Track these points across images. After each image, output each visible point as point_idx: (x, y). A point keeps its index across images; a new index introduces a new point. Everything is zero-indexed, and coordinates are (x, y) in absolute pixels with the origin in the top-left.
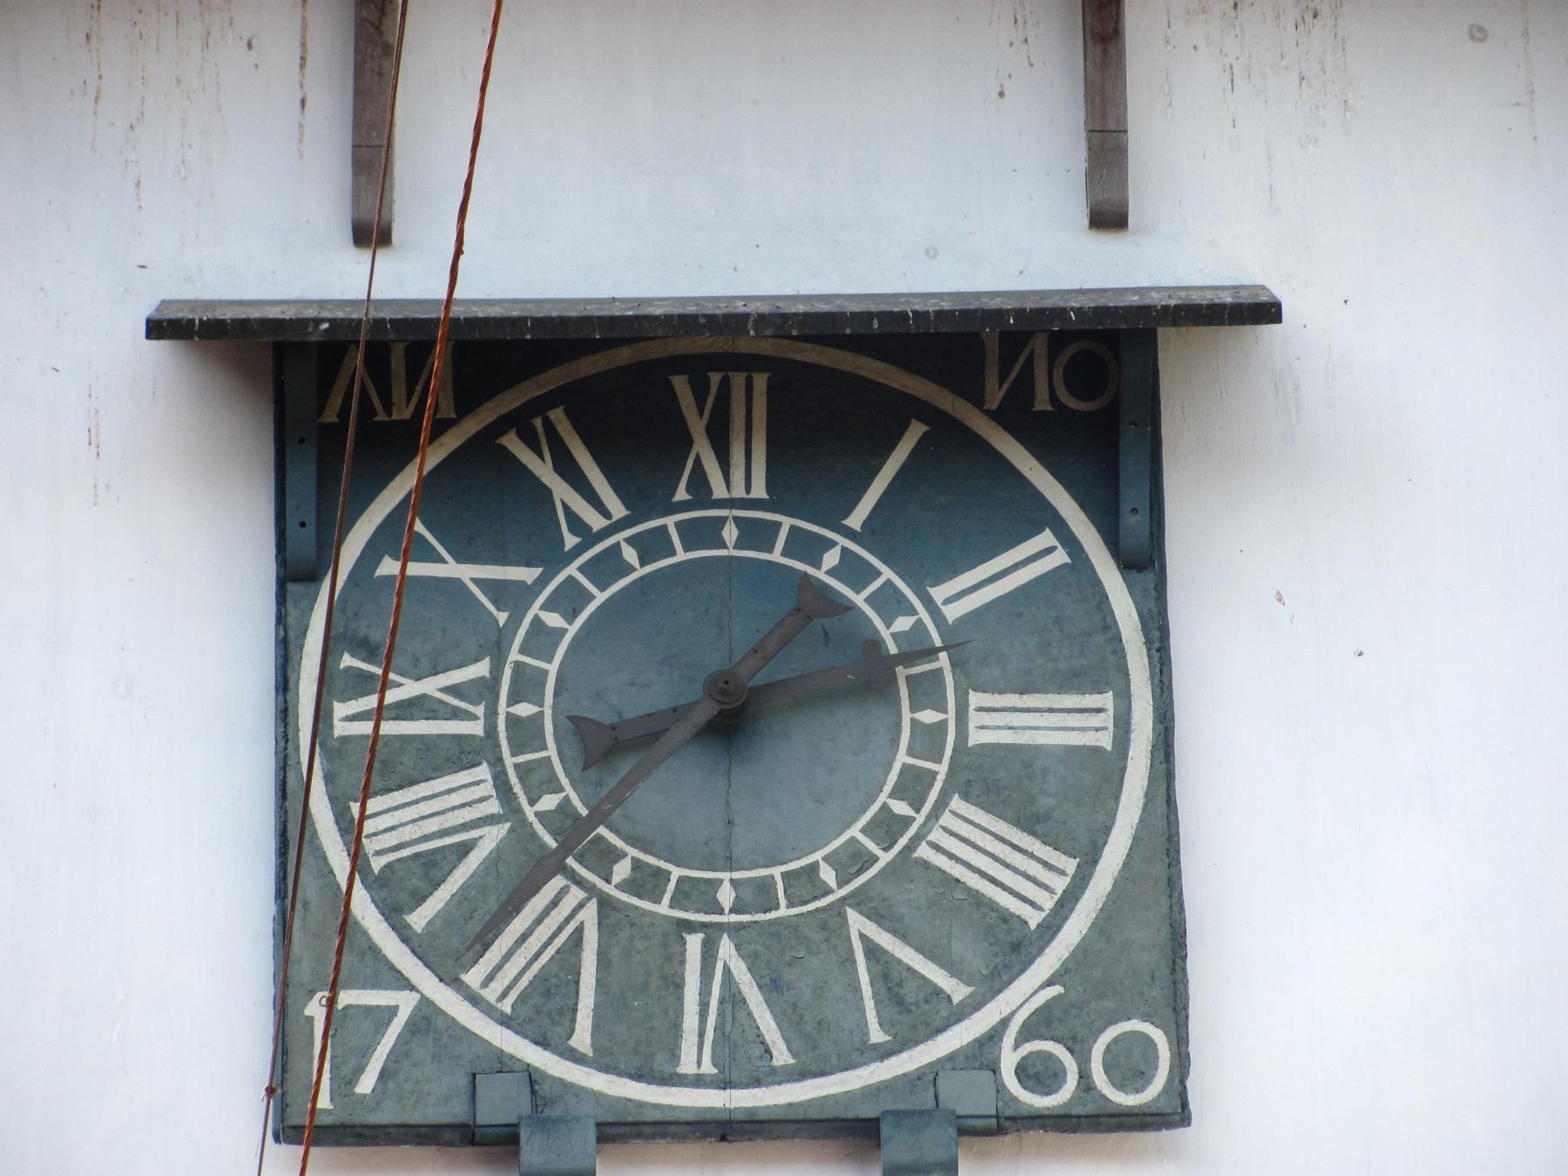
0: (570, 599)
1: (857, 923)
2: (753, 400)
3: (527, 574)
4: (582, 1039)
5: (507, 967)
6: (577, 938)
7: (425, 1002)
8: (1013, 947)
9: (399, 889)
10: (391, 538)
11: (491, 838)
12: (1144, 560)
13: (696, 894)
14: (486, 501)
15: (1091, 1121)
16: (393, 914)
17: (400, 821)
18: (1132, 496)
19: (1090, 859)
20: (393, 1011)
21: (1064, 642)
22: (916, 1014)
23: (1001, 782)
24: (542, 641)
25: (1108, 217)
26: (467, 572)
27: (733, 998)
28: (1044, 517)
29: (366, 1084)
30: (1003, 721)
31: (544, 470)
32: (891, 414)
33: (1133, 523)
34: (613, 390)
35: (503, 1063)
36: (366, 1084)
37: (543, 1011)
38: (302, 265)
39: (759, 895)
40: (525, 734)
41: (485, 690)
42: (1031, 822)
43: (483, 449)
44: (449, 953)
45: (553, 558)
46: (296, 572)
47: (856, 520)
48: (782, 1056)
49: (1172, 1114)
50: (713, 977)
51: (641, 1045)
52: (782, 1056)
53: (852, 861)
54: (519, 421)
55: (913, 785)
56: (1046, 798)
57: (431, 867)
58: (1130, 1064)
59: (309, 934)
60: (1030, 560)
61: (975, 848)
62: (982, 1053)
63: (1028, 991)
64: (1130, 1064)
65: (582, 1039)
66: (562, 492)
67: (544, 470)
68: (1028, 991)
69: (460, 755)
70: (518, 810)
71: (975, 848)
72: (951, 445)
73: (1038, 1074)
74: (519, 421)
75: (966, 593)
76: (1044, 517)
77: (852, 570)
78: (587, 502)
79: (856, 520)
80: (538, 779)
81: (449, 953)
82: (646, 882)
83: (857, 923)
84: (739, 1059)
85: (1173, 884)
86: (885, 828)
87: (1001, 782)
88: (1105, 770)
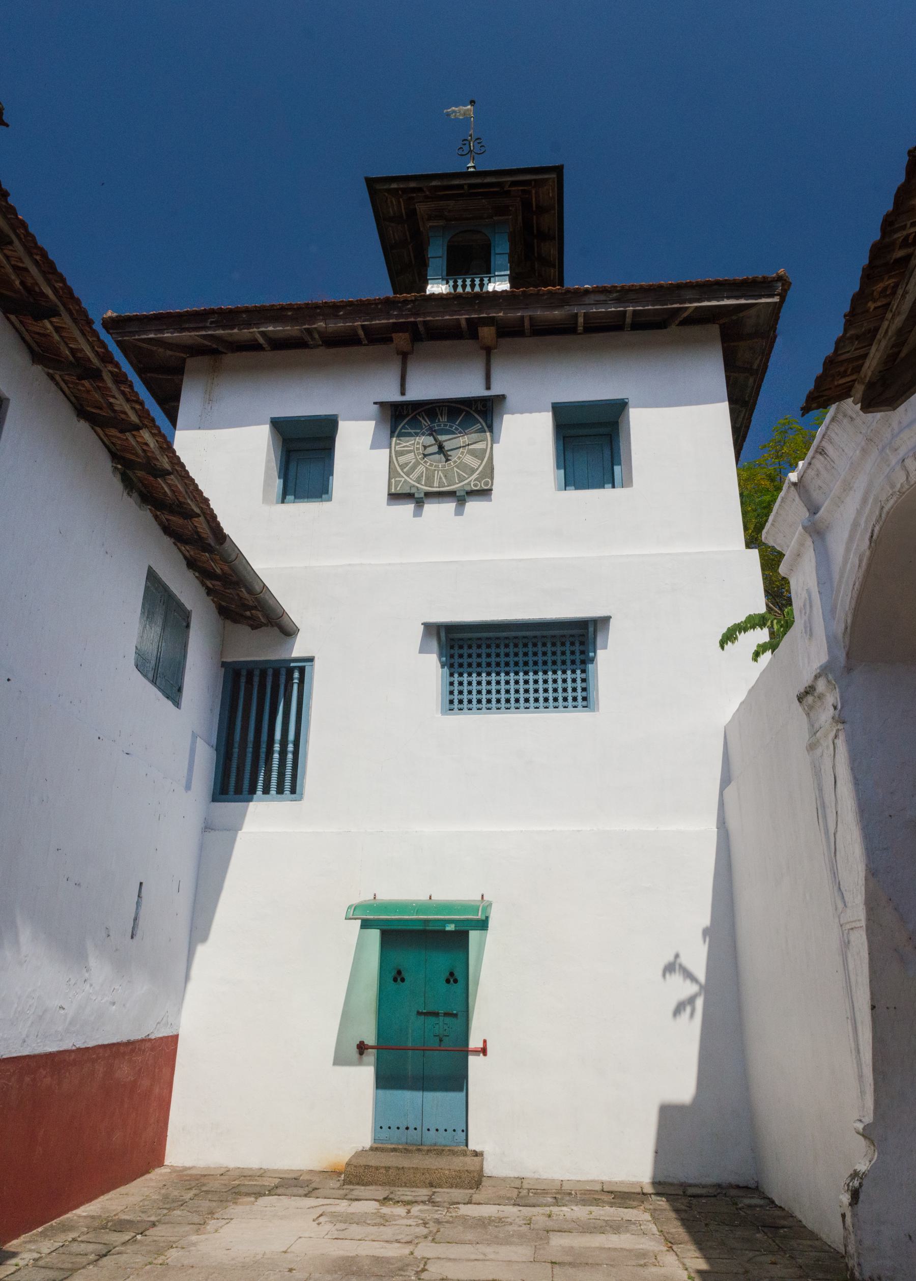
2: (445, 410)
7: (405, 481)
8: (473, 471)
9: (402, 467)
10: (404, 427)
11: (413, 461)
14: (415, 423)
16: (402, 470)
17: (402, 459)
18: (489, 419)
19: (482, 461)
23: (473, 453)
27: (440, 478)
32: (460, 412)
33: (489, 422)
35: (414, 486)
37: (418, 480)
38: (396, 397)
42: (476, 457)
43: (414, 418)
45: (422, 429)
51: (429, 482)
53: (455, 462)
54: (418, 414)
56: (479, 454)
57: (407, 464)
58: (486, 484)
59: (392, 473)
60: (478, 426)
61: (470, 460)
62: (469, 484)
63: (475, 476)
64: (486, 484)
66: (423, 421)
68: (475, 476)
69: (410, 452)
71: (470, 460)
72: (468, 413)
73: (475, 485)
74: (418, 414)
77: (456, 429)
78: (426, 423)
81: (408, 474)
82: (431, 465)
85: (492, 463)
86: (459, 458)
88: (485, 450)
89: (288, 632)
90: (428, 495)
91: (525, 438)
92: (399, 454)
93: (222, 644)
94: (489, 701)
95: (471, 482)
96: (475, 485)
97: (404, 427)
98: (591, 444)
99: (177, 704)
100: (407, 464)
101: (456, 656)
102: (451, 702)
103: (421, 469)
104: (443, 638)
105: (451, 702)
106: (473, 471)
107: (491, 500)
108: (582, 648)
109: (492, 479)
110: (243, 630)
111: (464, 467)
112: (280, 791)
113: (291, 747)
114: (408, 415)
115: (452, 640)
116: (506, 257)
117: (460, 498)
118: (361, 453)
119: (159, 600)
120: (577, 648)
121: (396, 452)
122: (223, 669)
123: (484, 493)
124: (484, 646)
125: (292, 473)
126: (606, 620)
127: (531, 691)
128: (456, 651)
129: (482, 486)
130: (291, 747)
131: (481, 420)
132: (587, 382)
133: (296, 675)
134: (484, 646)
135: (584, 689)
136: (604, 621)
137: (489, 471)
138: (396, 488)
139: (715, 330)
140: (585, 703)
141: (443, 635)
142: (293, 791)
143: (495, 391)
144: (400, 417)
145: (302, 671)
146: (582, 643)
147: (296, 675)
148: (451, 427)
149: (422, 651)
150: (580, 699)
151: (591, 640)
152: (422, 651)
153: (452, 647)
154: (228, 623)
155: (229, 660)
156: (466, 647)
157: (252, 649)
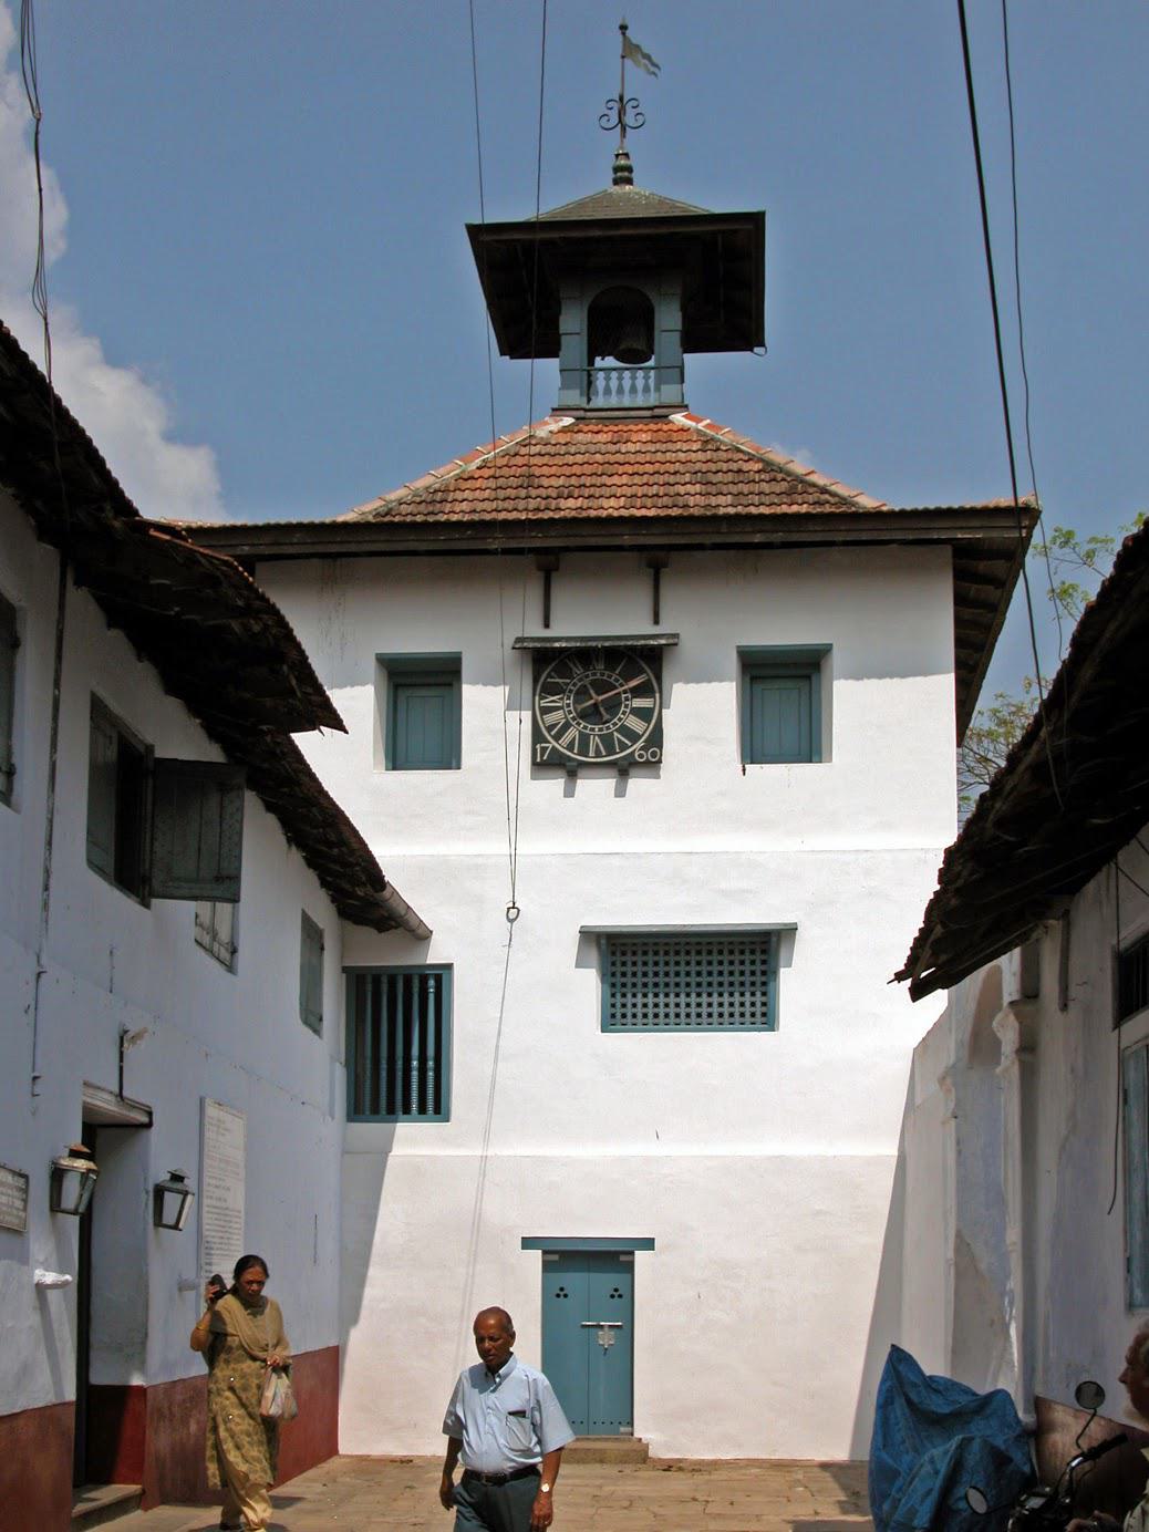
0: (574, 685)
1: (615, 733)
3: (568, 681)
4: (576, 751)
6: (574, 738)
7: (553, 747)
9: (550, 729)
10: (549, 676)
11: (564, 721)
13: (593, 730)
14: (564, 671)
15: (648, 763)
16: (549, 732)
17: (551, 718)
20: (547, 748)
22: (624, 747)
23: (638, 712)
24: (571, 691)
26: (560, 681)
27: (597, 746)
28: (645, 672)
29: (545, 758)
30: (638, 703)
31: (572, 665)
34: (584, 655)
36: (545, 758)
37: (570, 747)
38: (535, 630)
39: (601, 730)
40: (568, 705)
41: (562, 699)
44: (557, 738)
46: (535, 681)
47: (617, 672)
48: (604, 754)
49: (660, 761)
50: (594, 741)
51: (584, 751)
52: (604, 754)
54: (568, 657)
55: (624, 713)
56: (644, 714)
57: (554, 726)
59: (537, 737)
61: (635, 723)
63: (640, 743)
65: (576, 751)
66: (575, 669)
67: (572, 665)
68: (640, 743)
69: (558, 708)
70: (566, 717)
71: (635, 723)
73: (641, 756)
74: (568, 657)
75: (633, 683)
76: (642, 671)
77: (617, 681)
78: (578, 671)
79: (617, 672)
80: (570, 712)
81: (557, 741)
83: (615, 733)
84: (598, 754)
86: (620, 719)
87: (638, 712)
88: (652, 710)
89: (420, 935)
91: (701, 711)
92: (545, 711)
93: (344, 946)
94: (656, 1016)
96: (641, 756)
97: (549, 676)
100: (554, 726)
101: (618, 964)
102: (613, 1016)
103: (572, 733)
104: (604, 947)
105: (613, 1016)
106: (634, 737)
107: (658, 777)
108: (764, 957)
109: (661, 748)
110: (367, 933)
111: (625, 730)
114: (554, 660)
115: (614, 945)
117: (623, 770)
120: (758, 957)
121: (540, 708)
122: (344, 975)
124: (651, 953)
126: (790, 931)
127: (705, 1005)
128: (619, 958)
129: (648, 756)
131: (649, 671)
134: (651, 953)
135: (764, 1004)
136: (790, 931)
137: (656, 739)
138: (542, 756)
140: (764, 1019)
141: (603, 941)
144: (550, 666)
145: (438, 979)
146: (764, 952)
148: (610, 677)
149: (579, 965)
150: (758, 1014)
151: (773, 944)
152: (579, 965)
153: (613, 953)
154: (350, 926)
155: (347, 965)
156: (629, 954)
157: (382, 954)
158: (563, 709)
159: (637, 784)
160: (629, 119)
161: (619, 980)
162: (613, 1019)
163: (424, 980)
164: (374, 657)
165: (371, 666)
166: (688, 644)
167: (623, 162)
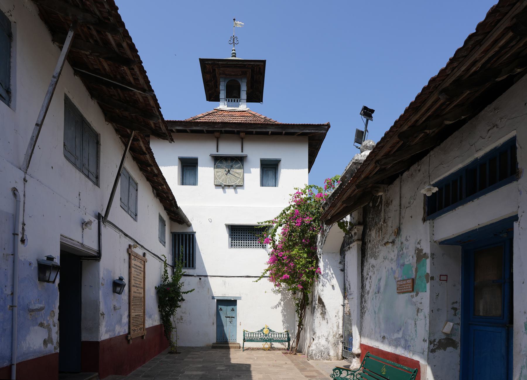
5: (221, 179)
12: (243, 165)
14: (221, 162)
17: (218, 174)
21: (240, 168)
25: (242, 152)
46: (215, 165)
59: (215, 178)
60: (239, 165)
75: (237, 166)
89: (189, 225)
90: (225, 186)
92: (217, 172)
93: (171, 227)
95: (237, 183)
98: (270, 169)
99: (164, 246)
103: (223, 177)
110: (176, 224)
112: (189, 266)
113: (191, 255)
116: (245, 92)
118: (206, 172)
119: (161, 220)
123: (241, 186)
125: (185, 175)
130: (191, 255)
132: (270, 152)
133: (191, 236)
139: (307, 137)
142: (193, 267)
143: (244, 153)
147: (191, 236)
154: (173, 222)
157: (180, 229)
158: (222, 172)
159: (239, 190)
160: (235, 42)
161: (233, 237)
162: (232, 246)
163: (189, 235)
164: (177, 159)
165: (177, 161)
166: (250, 157)
167: (234, 51)
